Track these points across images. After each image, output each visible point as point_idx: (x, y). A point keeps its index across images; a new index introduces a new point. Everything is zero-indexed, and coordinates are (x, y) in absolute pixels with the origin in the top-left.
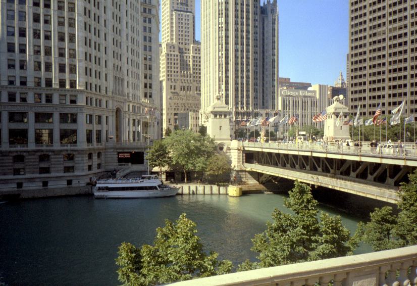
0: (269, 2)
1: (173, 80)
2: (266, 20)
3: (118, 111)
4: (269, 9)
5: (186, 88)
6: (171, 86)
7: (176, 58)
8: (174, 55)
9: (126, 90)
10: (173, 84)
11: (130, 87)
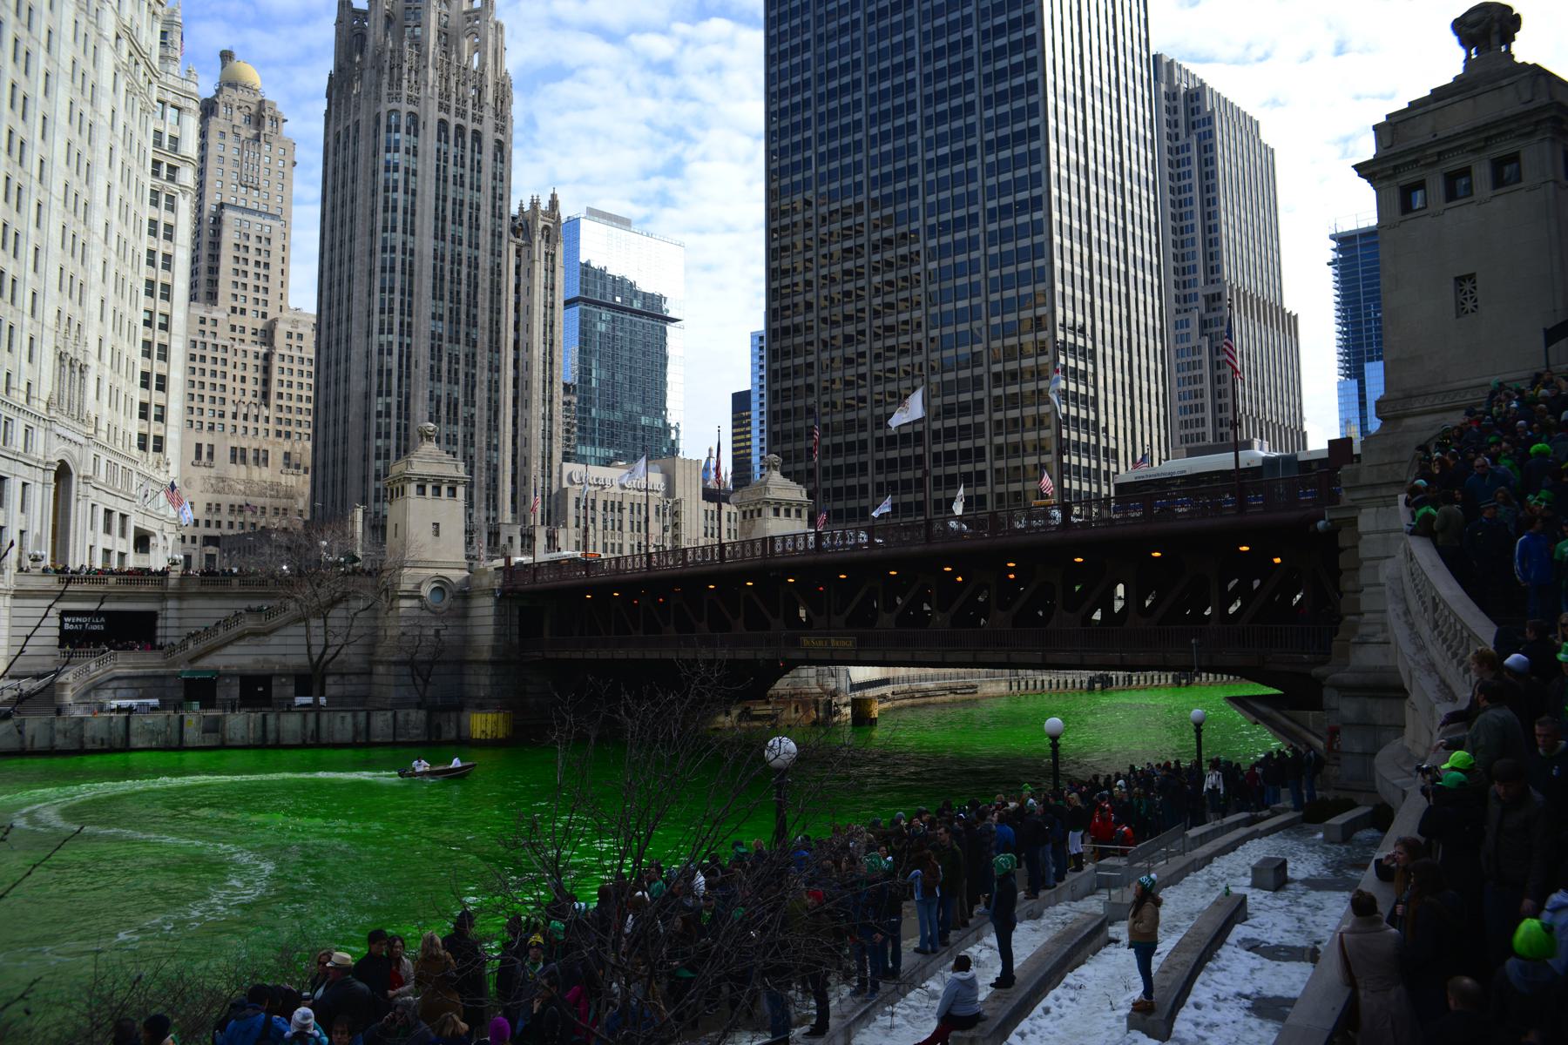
0: (535, 205)
1: (206, 426)
3: (63, 473)
5: (250, 455)
6: (199, 446)
7: (220, 355)
8: (216, 346)
9: (91, 405)
10: (206, 439)
11: (105, 397)
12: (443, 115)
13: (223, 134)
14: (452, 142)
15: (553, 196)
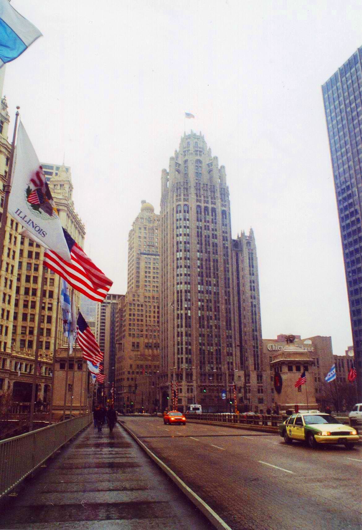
0: (243, 234)
2: (240, 255)
4: (244, 242)
6: (133, 343)
8: (138, 305)
10: (136, 340)
12: (198, 204)
13: (140, 228)
14: (203, 214)
15: (251, 229)
